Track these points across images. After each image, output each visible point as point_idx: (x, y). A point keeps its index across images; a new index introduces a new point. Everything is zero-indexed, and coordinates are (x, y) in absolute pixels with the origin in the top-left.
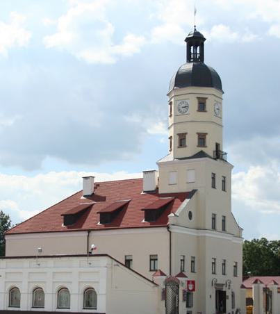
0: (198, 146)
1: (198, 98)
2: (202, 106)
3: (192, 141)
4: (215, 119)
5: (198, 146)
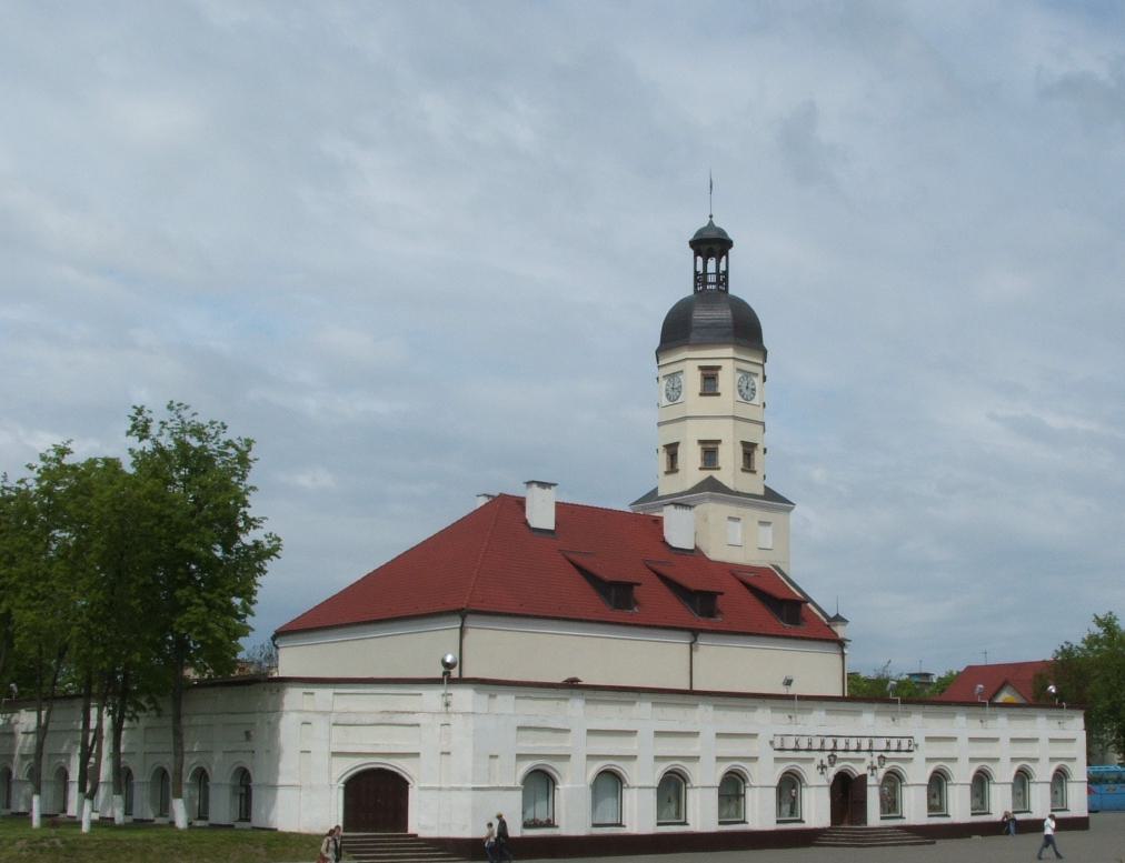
1: (701, 368)
3: (691, 457)
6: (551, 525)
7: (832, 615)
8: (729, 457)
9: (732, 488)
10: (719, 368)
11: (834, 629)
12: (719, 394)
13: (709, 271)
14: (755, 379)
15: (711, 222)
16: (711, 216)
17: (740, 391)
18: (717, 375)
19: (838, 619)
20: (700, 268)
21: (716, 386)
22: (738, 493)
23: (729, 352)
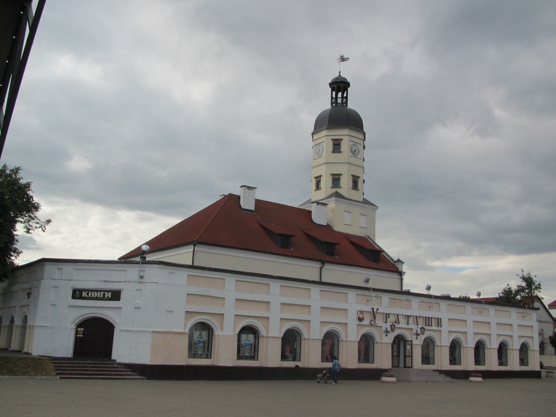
0: (332, 188)
1: (332, 139)
3: (326, 182)
4: (353, 160)
5: (332, 188)
6: (253, 208)
7: (395, 260)
8: (346, 182)
9: (346, 196)
10: (342, 139)
11: (396, 265)
12: (341, 152)
14: (359, 146)
15: (340, 75)
16: (340, 72)
17: (352, 151)
18: (341, 143)
19: (399, 261)
20: (334, 96)
21: (340, 148)
22: (350, 200)
23: (346, 132)
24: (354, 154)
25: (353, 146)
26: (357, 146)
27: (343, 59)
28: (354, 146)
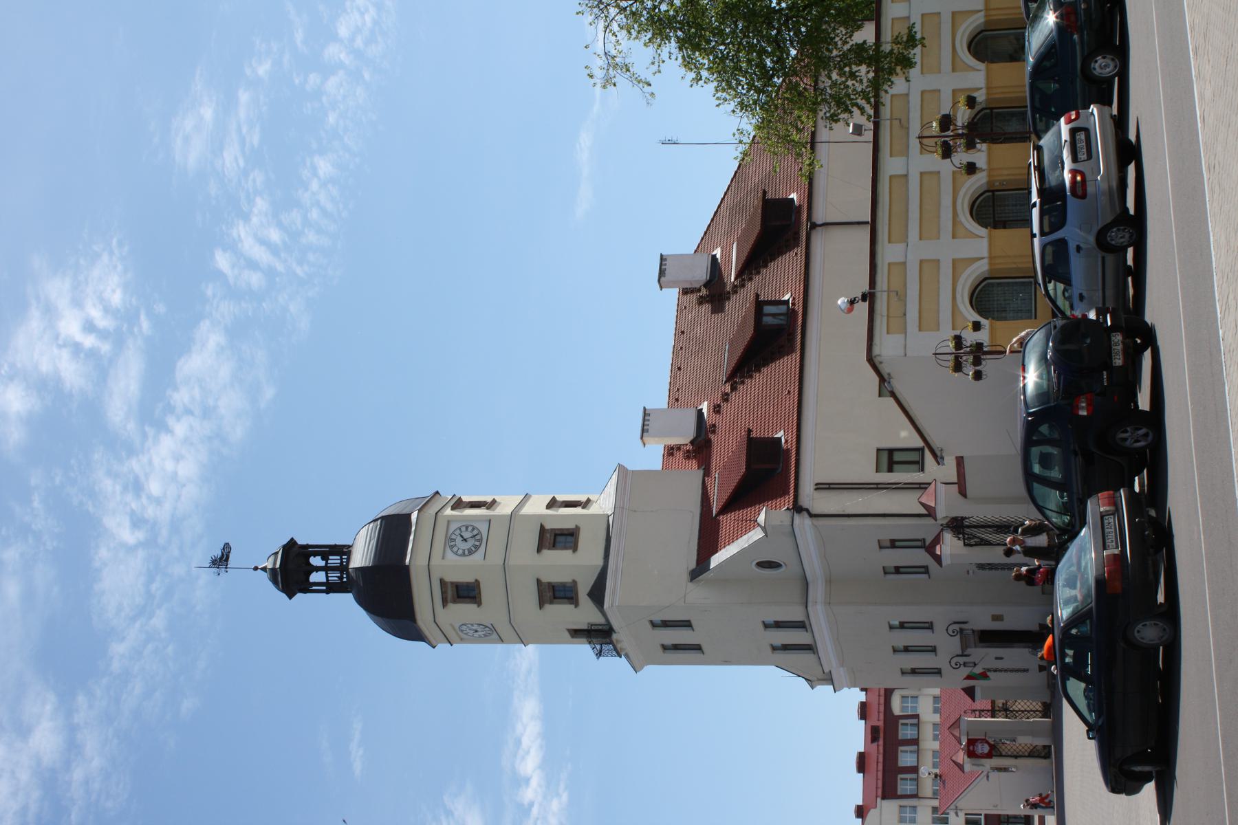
0: (577, 605)
2: (466, 593)
5: (577, 605)
10: (442, 582)
13: (324, 580)
17: (471, 552)
18: (452, 583)
24: (477, 543)
25: (455, 549)
26: (453, 533)
27: (222, 561)
28: (455, 545)
